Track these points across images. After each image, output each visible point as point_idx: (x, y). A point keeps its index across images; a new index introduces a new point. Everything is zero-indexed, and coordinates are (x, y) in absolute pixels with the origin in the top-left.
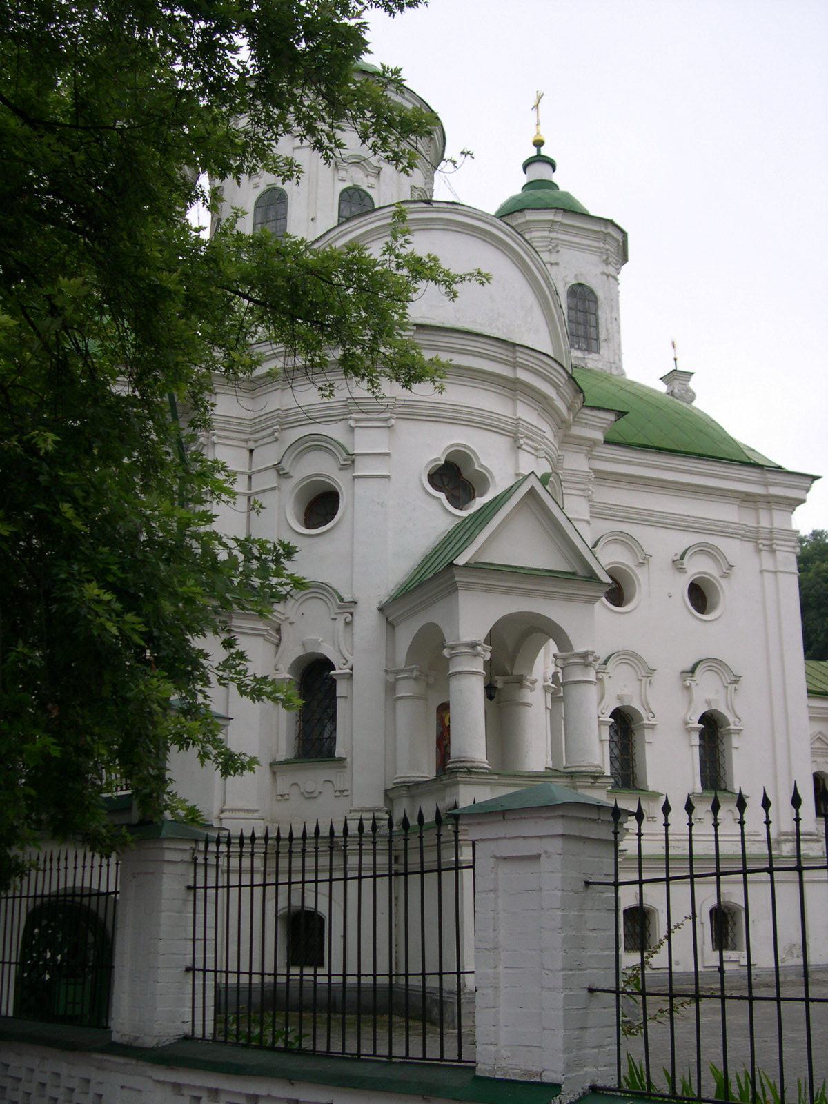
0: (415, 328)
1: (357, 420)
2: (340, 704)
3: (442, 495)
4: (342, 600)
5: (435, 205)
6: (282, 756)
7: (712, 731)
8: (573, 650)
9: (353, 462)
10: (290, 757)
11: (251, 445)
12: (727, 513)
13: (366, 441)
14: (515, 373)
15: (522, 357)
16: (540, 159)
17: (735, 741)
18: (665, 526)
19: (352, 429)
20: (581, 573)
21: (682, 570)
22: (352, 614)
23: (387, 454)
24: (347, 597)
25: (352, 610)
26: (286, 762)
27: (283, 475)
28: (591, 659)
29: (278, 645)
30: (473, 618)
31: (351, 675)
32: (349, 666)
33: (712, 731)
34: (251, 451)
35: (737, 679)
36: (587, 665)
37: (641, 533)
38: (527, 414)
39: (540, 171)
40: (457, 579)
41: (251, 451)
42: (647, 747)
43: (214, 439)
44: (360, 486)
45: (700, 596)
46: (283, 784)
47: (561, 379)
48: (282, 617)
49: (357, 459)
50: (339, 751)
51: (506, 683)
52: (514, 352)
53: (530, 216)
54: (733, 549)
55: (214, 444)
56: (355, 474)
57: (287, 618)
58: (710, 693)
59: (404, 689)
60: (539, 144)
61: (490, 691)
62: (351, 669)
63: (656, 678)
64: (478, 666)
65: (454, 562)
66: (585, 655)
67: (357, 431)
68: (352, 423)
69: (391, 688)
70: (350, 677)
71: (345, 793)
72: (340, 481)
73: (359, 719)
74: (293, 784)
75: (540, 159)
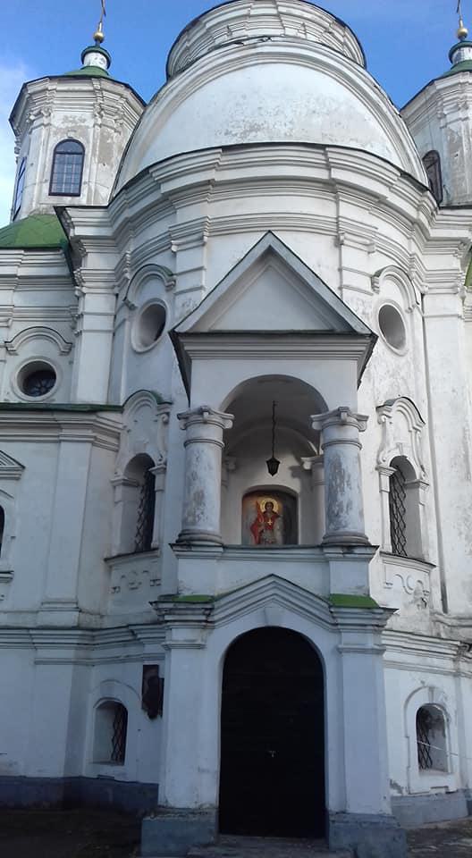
0: (220, 150)
1: (178, 245)
2: (158, 496)
4: (160, 402)
5: (245, 43)
6: (114, 553)
8: (328, 410)
9: (175, 281)
10: (123, 551)
11: (116, 290)
13: (184, 261)
14: (418, 215)
15: (333, 156)
19: (175, 253)
20: (338, 328)
22: (168, 414)
23: (201, 269)
24: (166, 399)
25: (168, 410)
27: (132, 308)
28: (344, 415)
29: (117, 451)
31: (165, 469)
32: (164, 460)
34: (117, 295)
36: (344, 424)
38: (351, 211)
40: (186, 348)
41: (117, 295)
43: (84, 290)
44: (180, 300)
46: (115, 579)
47: (393, 177)
48: (121, 426)
49: (178, 279)
50: (153, 544)
51: (314, 463)
52: (325, 154)
55: (84, 294)
56: (178, 290)
57: (125, 427)
62: (165, 464)
64: (215, 433)
65: (176, 330)
66: (338, 413)
67: (179, 255)
68: (174, 248)
71: (158, 583)
74: (123, 577)
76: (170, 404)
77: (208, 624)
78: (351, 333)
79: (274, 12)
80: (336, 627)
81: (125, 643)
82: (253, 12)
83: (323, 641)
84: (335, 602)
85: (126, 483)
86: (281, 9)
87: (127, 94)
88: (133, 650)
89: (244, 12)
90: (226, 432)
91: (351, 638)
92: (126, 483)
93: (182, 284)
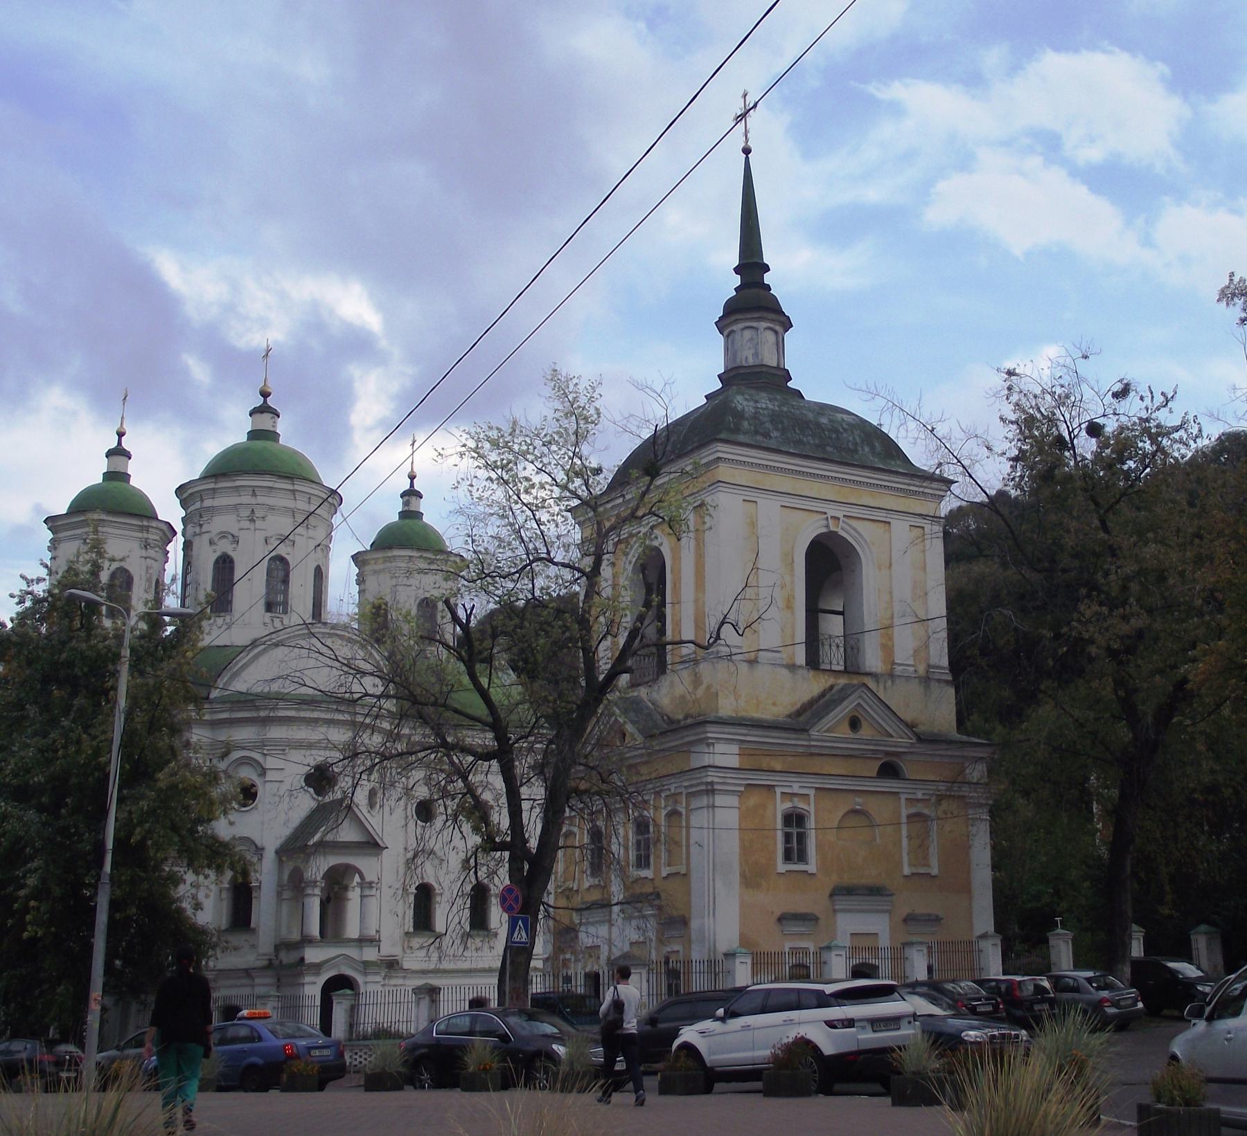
2: (254, 901)
3: (311, 790)
6: (223, 928)
24: (259, 843)
26: (226, 931)
30: (318, 867)
50: (253, 925)
53: (396, 552)
59: (286, 895)
60: (412, 477)
61: (323, 905)
64: (317, 891)
66: (371, 883)
69: (279, 894)
70: (259, 887)
72: (258, 781)
73: (264, 909)
76: (263, 849)
77: (318, 974)
78: (376, 845)
79: (290, 487)
80: (365, 974)
81: (239, 978)
82: (276, 485)
83: (360, 979)
84: (366, 964)
85: (228, 889)
86: (296, 487)
87: (165, 528)
88: (244, 981)
89: (270, 484)
90: (322, 890)
91: (370, 978)
92: (228, 889)
93: (270, 776)
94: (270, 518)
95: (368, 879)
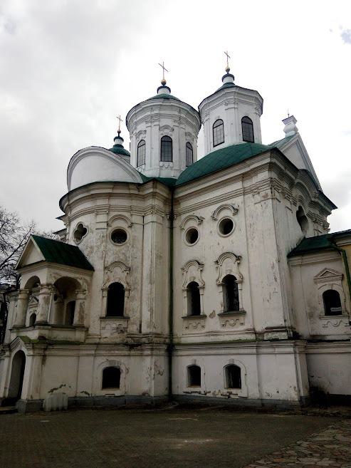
7: (230, 285)
12: (238, 186)
16: (228, 75)
17: (239, 286)
18: (205, 206)
21: (215, 220)
33: (230, 285)
35: (239, 258)
37: (199, 213)
39: (227, 80)
42: (201, 297)
45: (227, 227)
54: (237, 201)
58: (229, 267)
63: (206, 266)
75: (228, 75)
94: (138, 127)
95: (41, 283)
